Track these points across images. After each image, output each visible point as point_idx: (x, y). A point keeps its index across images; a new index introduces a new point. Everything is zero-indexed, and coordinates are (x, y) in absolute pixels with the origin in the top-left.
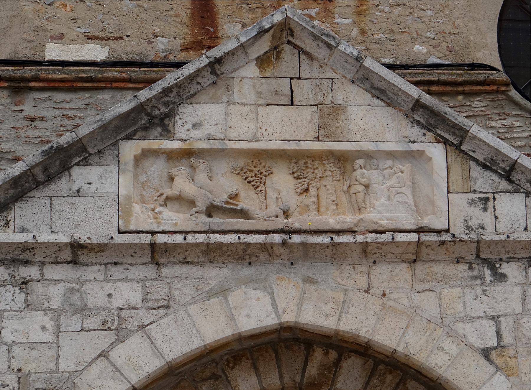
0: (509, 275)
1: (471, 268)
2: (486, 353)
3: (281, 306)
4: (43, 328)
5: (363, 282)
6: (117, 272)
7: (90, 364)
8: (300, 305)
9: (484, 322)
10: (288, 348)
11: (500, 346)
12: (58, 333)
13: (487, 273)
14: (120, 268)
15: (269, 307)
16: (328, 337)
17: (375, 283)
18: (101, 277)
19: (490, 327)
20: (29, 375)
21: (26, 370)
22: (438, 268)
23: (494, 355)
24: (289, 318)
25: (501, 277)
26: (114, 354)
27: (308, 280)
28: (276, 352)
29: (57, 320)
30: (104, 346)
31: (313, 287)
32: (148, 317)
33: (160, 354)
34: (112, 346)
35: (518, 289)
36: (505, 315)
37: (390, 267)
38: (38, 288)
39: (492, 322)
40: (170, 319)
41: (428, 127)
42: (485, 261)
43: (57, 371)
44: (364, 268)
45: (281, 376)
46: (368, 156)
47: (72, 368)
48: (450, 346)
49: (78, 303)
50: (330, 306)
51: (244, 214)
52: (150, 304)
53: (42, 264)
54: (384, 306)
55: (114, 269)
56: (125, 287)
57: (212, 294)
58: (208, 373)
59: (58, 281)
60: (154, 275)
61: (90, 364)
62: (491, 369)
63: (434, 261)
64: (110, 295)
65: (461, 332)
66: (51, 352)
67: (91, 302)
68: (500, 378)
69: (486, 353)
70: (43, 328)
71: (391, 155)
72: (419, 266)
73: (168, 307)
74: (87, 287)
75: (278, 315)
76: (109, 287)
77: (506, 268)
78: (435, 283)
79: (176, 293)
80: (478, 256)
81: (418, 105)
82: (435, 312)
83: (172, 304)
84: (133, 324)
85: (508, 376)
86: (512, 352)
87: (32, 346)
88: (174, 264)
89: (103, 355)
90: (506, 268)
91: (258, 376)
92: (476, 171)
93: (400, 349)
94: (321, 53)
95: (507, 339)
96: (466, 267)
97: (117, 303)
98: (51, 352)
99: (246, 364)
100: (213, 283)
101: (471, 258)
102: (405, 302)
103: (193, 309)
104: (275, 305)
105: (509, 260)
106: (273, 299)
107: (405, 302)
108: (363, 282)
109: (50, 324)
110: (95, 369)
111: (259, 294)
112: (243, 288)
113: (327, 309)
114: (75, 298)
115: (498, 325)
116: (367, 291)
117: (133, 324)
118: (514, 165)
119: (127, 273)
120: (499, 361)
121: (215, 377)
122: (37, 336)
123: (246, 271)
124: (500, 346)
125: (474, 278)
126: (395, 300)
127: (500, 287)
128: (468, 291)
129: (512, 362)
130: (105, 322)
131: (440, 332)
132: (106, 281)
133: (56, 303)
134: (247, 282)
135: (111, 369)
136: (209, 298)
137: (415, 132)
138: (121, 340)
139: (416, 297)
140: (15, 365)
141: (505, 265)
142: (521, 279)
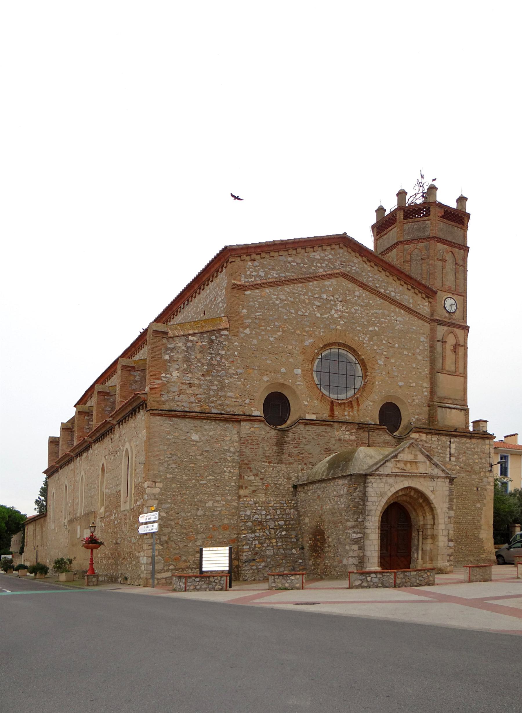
24: (410, 485)
25: (434, 480)
38: (382, 479)
41: (427, 458)
46: (419, 462)
51: (405, 470)
71: (422, 462)
77: (435, 479)
81: (427, 455)
87: (381, 488)
90: (435, 479)
92: (432, 465)
94: (416, 446)
97: (391, 482)
118: (438, 464)
123: (405, 478)
133: (384, 482)
134: (405, 480)
137: (425, 459)
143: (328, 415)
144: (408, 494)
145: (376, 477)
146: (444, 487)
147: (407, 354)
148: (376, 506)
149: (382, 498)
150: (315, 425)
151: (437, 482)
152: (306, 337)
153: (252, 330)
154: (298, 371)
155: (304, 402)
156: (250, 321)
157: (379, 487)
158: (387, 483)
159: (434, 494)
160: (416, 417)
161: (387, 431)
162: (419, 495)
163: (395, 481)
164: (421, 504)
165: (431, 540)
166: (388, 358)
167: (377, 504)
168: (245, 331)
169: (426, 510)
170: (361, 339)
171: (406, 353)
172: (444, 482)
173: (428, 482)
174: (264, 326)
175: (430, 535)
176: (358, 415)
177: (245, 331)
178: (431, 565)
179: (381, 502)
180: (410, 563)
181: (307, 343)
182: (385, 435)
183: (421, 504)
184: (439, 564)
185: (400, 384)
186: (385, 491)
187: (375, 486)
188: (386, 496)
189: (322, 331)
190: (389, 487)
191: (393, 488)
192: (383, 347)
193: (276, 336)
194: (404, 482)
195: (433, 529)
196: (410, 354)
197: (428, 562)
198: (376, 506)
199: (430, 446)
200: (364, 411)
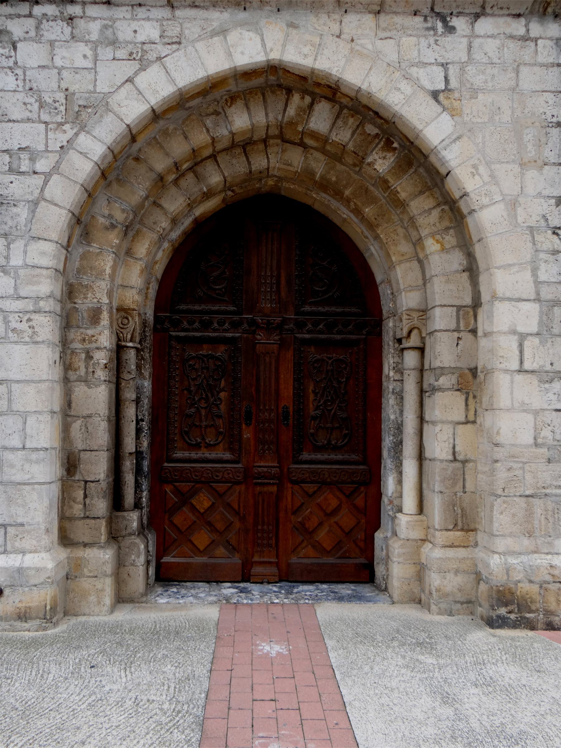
0: (458, 28)
1: (425, 20)
2: (435, 95)
3: (269, 45)
4: (85, 56)
5: (335, 28)
6: (141, 12)
7: (119, 87)
8: (284, 46)
9: (435, 68)
11: (447, 89)
12: (95, 61)
13: (439, 25)
14: (143, 9)
15: (259, 46)
17: (346, 30)
18: (128, 16)
19: (439, 73)
20: (74, 94)
21: (71, 90)
22: (398, 20)
23: (441, 97)
24: (275, 56)
25: (451, 30)
26: (138, 80)
27: (292, 25)
29: (95, 49)
30: (130, 73)
31: (295, 31)
32: (164, 50)
33: (173, 81)
34: (136, 74)
35: (465, 41)
36: (453, 63)
37: (359, 16)
38: (81, 24)
39: (441, 69)
40: (181, 52)
42: (438, 14)
43: (95, 92)
44: (336, 16)
47: (106, 90)
48: (406, 87)
49: (111, 37)
50: (309, 47)
52: (166, 40)
53: (84, 3)
54: (352, 49)
55: (139, 10)
56: (147, 24)
57: (214, 34)
58: (211, 110)
59: (95, 19)
60: (170, 16)
61: (119, 87)
62: (439, 109)
63: (395, 13)
64: (135, 32)
65: (415, 75)
66: (91, 77)
67: (121, 36)
68: (445, 117)
69: (435, 95)
70: (85, 56)
72: (382, 17)
73: (180, 43)
74: (118, 24)
75: (266, 54)
76: (135, 25)
77: (455, 22)
78: (395, 32)
79: (187, 32)
80: (432, 9)
82: (394, 57)
83: (183, 41)
84: (152, 56)
85: (452, 116)
86: (457, 95)
87: (76, 70)
88: (185, 7)
89: (130, 80)
90: (455, 22)
91: (249, 114)
93: (364, 87)
95: (453, 83)
96: (422, 19)
97: (141, 38)
98: (91, 77)
99: (240, 103)
100: (215, 24)
101: (426, 11)
102: (370, 47)
103: (200, 45)
104: (264, 45)
105: (459, 14)
106: (263, 40)
107: (370, 47)
108: (335, 28)
109: (89, 53)
110: (123, 92)
111: (252, 34)
112: (239, 30)
113: (306, 50)
114: (109, 32)
115: (446, 71)
116: (338, 37)
117: (152, 56)
119: (148, 14)
120: (445, 102)
121: (217, 113)
122: (80, 63)
123: (242, 15)
124: (447, 89)
125: (428, 29)
126: (362, 46)
127: (450, 38)
128: (422, 40)
129: (456, 104)
130: (131, 54)
131: (397, 74)
132: (133, 19)
133: (94, 36)
134: (242, 24)
135: (136, 92)
136: (212, 37)
138: (143, 68)
139: (379, 43)
140: (64, 85)
141: (454, 19)
142: (468, 32)
144: (292, 124)
145: (38, 10)
146: (524, 71)
148: (38, 181)
149: (83, 128)
151: (473, 36)
157: (60, 70)
158: (114, 43)
159: (454, 113)
162: (371, 129)
163: (173, 31)
164: (384, 183)
165: (460, 398)
167: (42, 165)
169: (421, 221)
172: (525, 39)
173: (408, 41)
175: (452, 370)
178: (461, 553)
179: (73, 155)
180: (377, 525)
184: (495, 561)
186: (103, 87)
187: (33, 62)
188: (109, 118)
190: (130, 68)
191: (154, 71)
194: (233, 37)
195: (474, 332)
197: (440, 537)
198: (38, 181)
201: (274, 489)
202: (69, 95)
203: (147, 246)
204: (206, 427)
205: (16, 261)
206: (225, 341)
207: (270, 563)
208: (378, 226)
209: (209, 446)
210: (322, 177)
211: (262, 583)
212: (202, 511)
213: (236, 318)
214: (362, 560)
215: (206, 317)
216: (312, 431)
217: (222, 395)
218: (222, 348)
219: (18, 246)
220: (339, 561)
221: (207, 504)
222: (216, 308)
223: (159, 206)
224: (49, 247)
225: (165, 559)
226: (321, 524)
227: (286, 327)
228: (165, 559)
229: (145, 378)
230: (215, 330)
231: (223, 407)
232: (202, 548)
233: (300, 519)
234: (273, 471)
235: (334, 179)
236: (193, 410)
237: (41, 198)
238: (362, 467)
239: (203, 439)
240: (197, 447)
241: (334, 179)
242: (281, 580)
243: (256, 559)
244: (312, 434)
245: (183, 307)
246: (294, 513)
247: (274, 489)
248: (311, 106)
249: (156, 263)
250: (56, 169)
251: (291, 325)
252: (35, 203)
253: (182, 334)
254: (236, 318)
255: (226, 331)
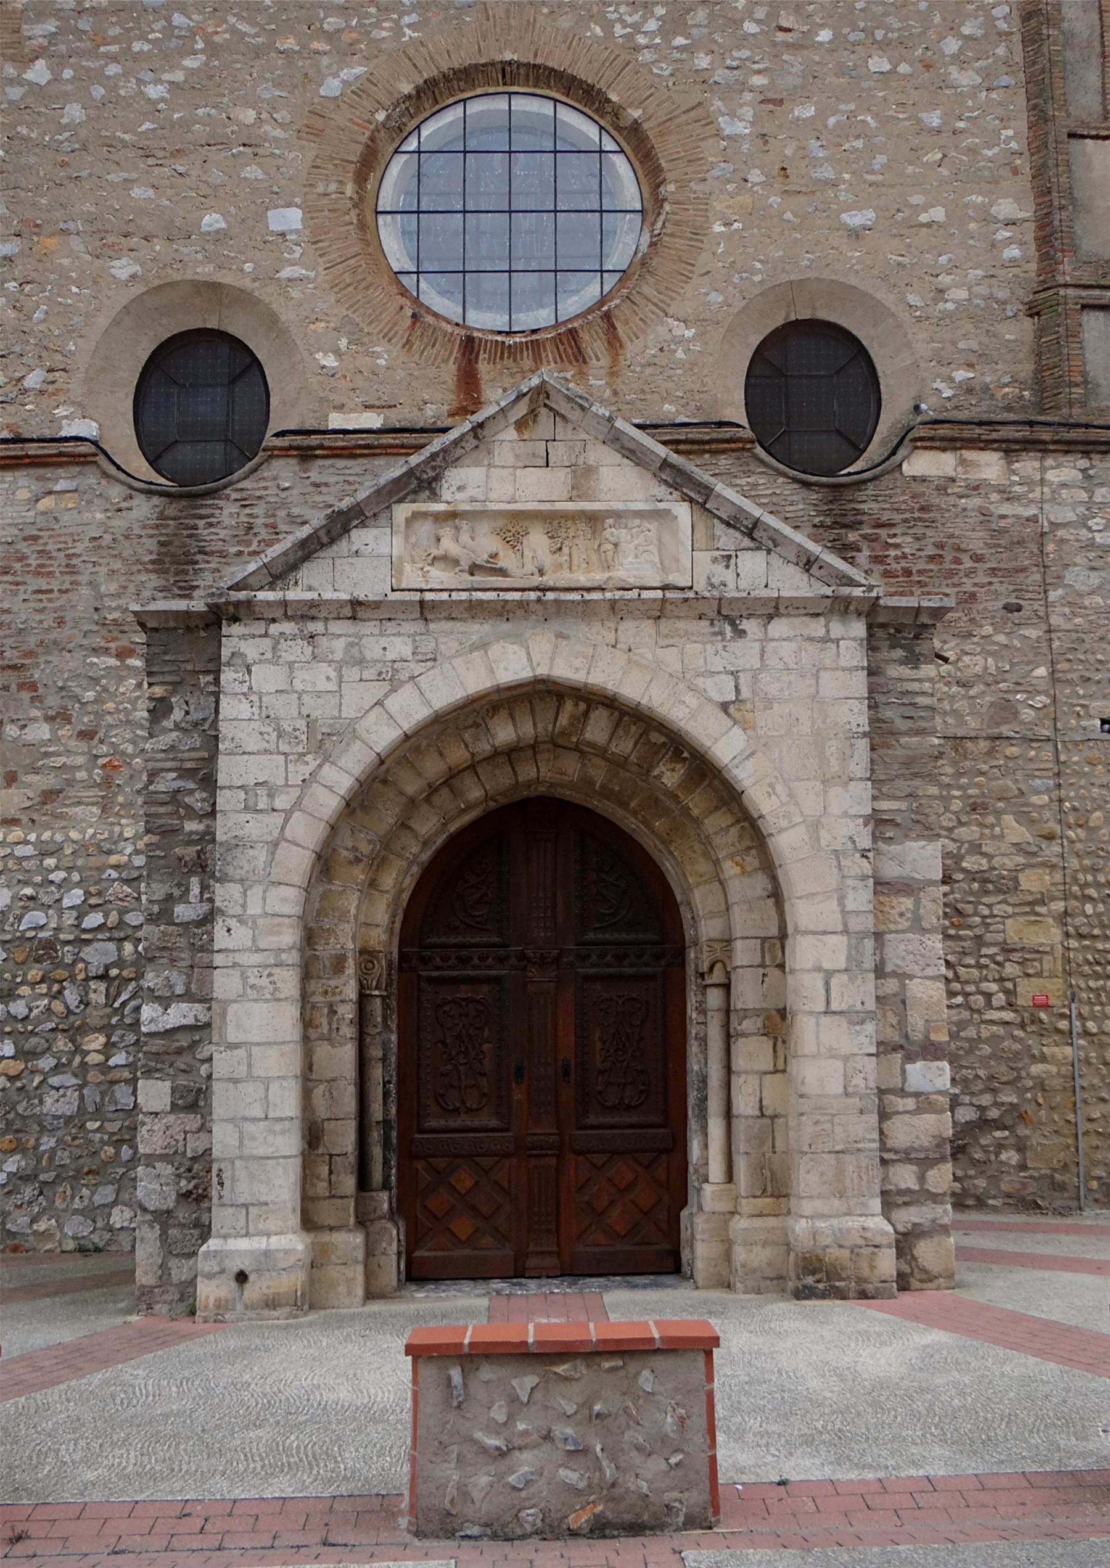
0: (749, 632)
1: (712, 624)
2: (725, 707)
3: (536, 659)
4: (328, 678)
5: (610, 637)
6: (391, 627)
7: (368, 711)
8: (552, 659)
9: (723, 677)
10: (541, 699)
11: (738, 700)
12: (340, 682)
13: (728, 629)
14: (393, 623)
15: (525, 660)
16: (578, 689)
17: (621, 639)
18: (376, 631)
19: (729, 682)
20: (316, 720)
21: (313, 717)
22: (680, 625)
24: (542, 671)
25: (741, 634)
26: (388, 703)
27: (560, 636)
28: (531, 703)
29: (339, 671)
30: (380, 696)
31: (565, 642)
32: (418, 669)
33: (428, 703)
34: (386, 696)
35: (757, 645)
36: (743, 670)
37: (636, 623)
38: (323, 642)
39: (731, 677)
40: (437, 671)
42: (726, 617)
43: (340, 717)
44: (612, 625)
45: (535, 725)
47: (353, 715)
48: (691, 700)
49: (357, 655)
50: (581, 659)
52: (420, 657)
53: (326, 619)
54: (629, 661)
55: (388, 624)
56: (397, 640)
57: (474, 648)
59: (340, 636)
60: (423, 630)
61: (368, 711)
63: (678, 617)
64: (385, 649)
65: (701, 686)
66: (334, 701)
67: (368, 655)
69: (725, 707)
70: (328, 678)
72: (663, 621)
73: (435, 660)
74: (364, 641)
75: (533, 669)
76: (384, 641)
77: (745, 625)
78: (677, 639)
79: (442, 647)
80: (719, 612)
82: (678, 667)
83: (439, 657)
84: (404, 676)
86: (749, 706)
87: (319, 694)
88: (440, 619)
89: (379, 703)
90: (745, 625)
94: (574, 415)
95: (745, 693)
96: (708, 623)
97: (391, 655)
98: (334, 701)
100: (474, 637)
101: (713, 614)
102: (649, 656)
103: (456, 662)
104: (530, 659)
105: (750, 616)
106: (528, 653)
107: (649, 656)
108: (610, 637)
109: (333, 675)
110: (372, 716)
111: (515, 647)
112: (502, 643)
113: (578, 663)
114: (355, 651)
115: (737, 679)
116: (614, 646)
117: (404, 676)
119: (399, 628)
120: (737, 715)
122: (323, 685)
123: (505, 627)
124: (738, 700)
125: (715, 634)
126: (640, 655)
127: (740, 643)
128: (709, 646)
129: (749, 716)
130: (380, 673)
131: (681, 686)
132: (382, 635)
133: (338, 656)
134: (505, 637)
135: (386, 716)
136: (471, 652)
138: (393, 690)
139: (659, 652)
140: (305, 712)
141: (745, 621)
142: (761, 635)
143: (446, 408)
145: (274, 629)
146: (825, 676)
147: (886, 67)
149: (327, 759)
150: (354, 456)
151: (767, 639)
152: (325, 61)
153: (58, 62)
154: (288, 219)
155: (319, 356)
156: (51, 26)
158: (361, 662)
159: (746, 726)
160: (961, 375)
161: (759, 450)
162: (656, 738)
163: (427, 646)
166: (780, 102)
167: (282, 802)
168: (29, 75)
169: (717, 840)
170: (619, 30)
171: (879, 63)
172: (825, 640)
173: (690, 648)
174: (115, 40)
176: (615, 393)
177: (29, 75)
179: (316, 789)
180: (684, 1203)
181: (332, 87)
182: (749, 473)
183: (677, 796)
185: (854, 219)
186: (348, 712)
189: (407, 20)
190: (378, 690)
191: (407, 690)
192: (746, 53)
193: (179, 76)
194: (494, 651)
195: (782, 966)
196: (904, 68)
197: (746, 1206)
199: (1032, 511)
200: (649, 371)
201: (553, 1161)
202: (311, 723)
203: (394, 876)
204: (466, 1087)
205: (254, 909)
206: (489, 980)
207: (550, 1253)
208: (671, 842)
209: (470, 1111)
210: (602, 786)
211: (539, 1277)
212: (463, 1192)
213: (502, 952)
214: (666, 1246)
215: (464, 953)
216: (599, 1088)
217: (486, 1047)
218: (485, 988)
219: (255, 893)
220: (638, 1248)
221: (469, 1183)
222: (476, 940)
223: (409, 828)
224: (291, 893)
225: (417, 1254)
226: (612, 1203)
227: (565, 960)
228: (417, 1254)
229: (391, 1031)
230: (475, 968)
231: (486, 1062)
232: (463, 1238)
233: (586, 1198)
234: (552, 1139)
235: (617, 788)
236: (450, 1067)
237: (282, 838)
238: (662, 1130)
239: (463, 1102)
240: (457, 1111)
241: (617, 788)
242: (562, 1275)
243: (531, 1248)
244: (600, 1092)
245: (434, 940)
246: (578, 1191)
247: (553, 1161)
248: (586, 714)
249: (403, 891)
250: (297, 805)
251: (571, 959)
252: (276, 844)
253: (435, 974)
254: (502, 952)
255: (489, 967)
